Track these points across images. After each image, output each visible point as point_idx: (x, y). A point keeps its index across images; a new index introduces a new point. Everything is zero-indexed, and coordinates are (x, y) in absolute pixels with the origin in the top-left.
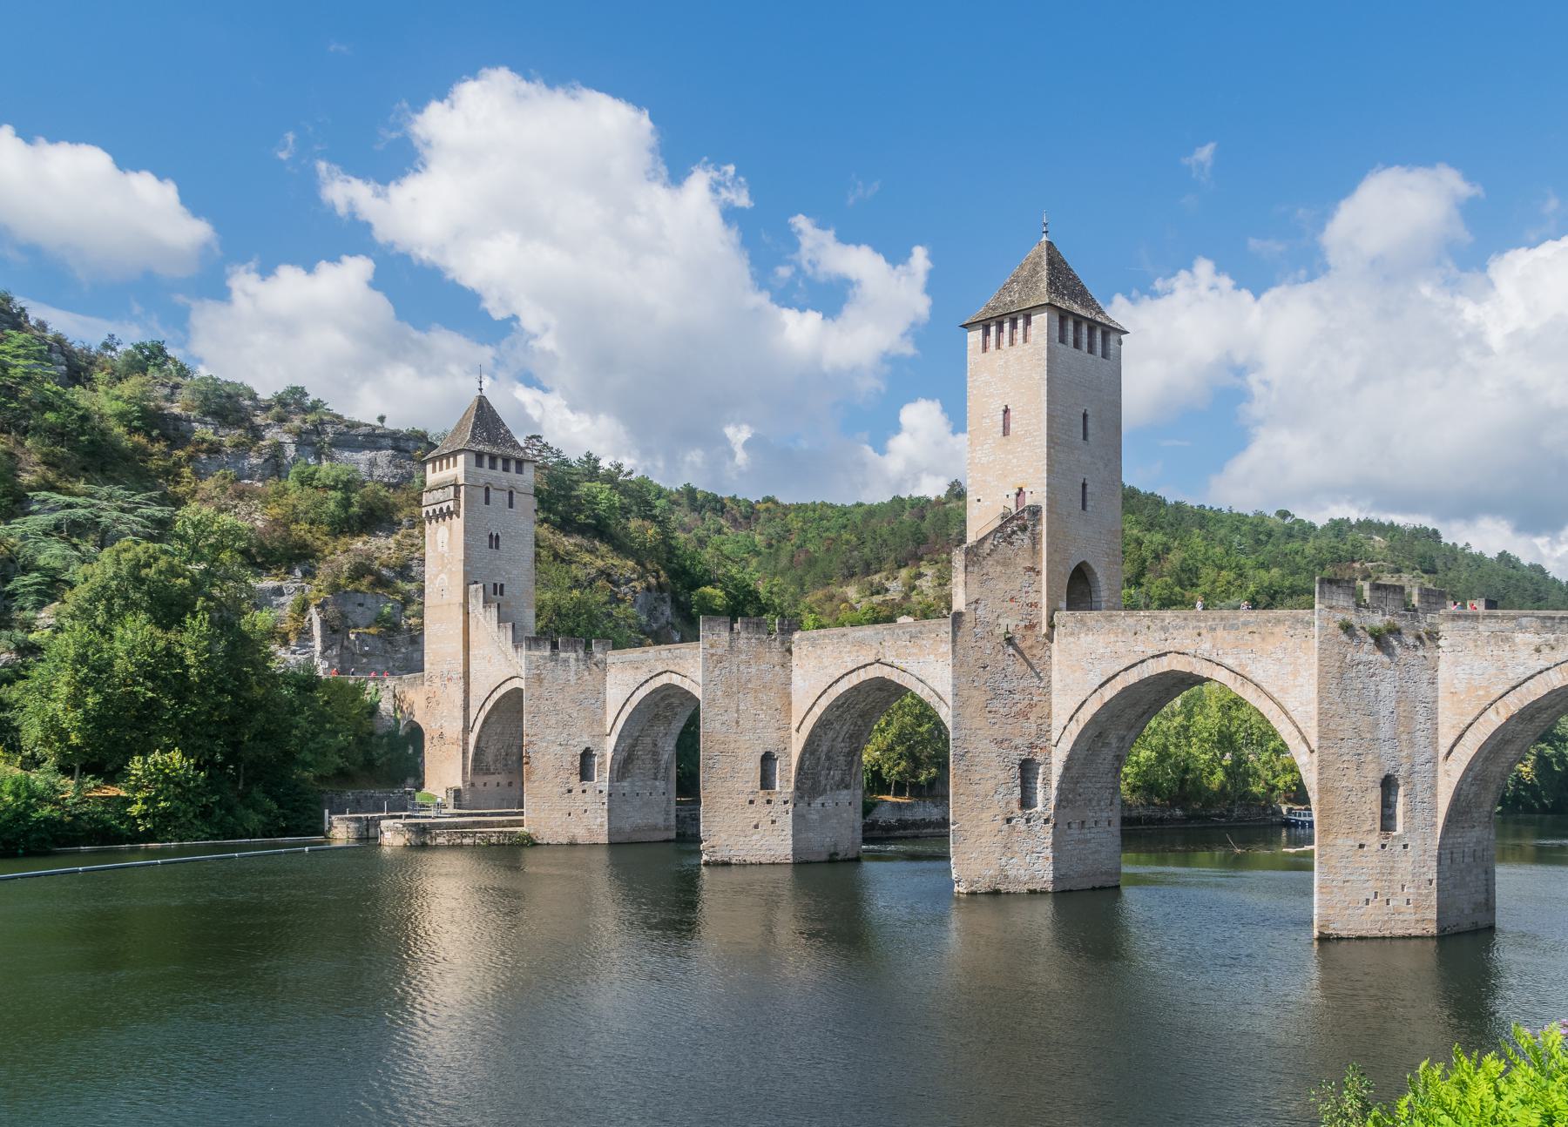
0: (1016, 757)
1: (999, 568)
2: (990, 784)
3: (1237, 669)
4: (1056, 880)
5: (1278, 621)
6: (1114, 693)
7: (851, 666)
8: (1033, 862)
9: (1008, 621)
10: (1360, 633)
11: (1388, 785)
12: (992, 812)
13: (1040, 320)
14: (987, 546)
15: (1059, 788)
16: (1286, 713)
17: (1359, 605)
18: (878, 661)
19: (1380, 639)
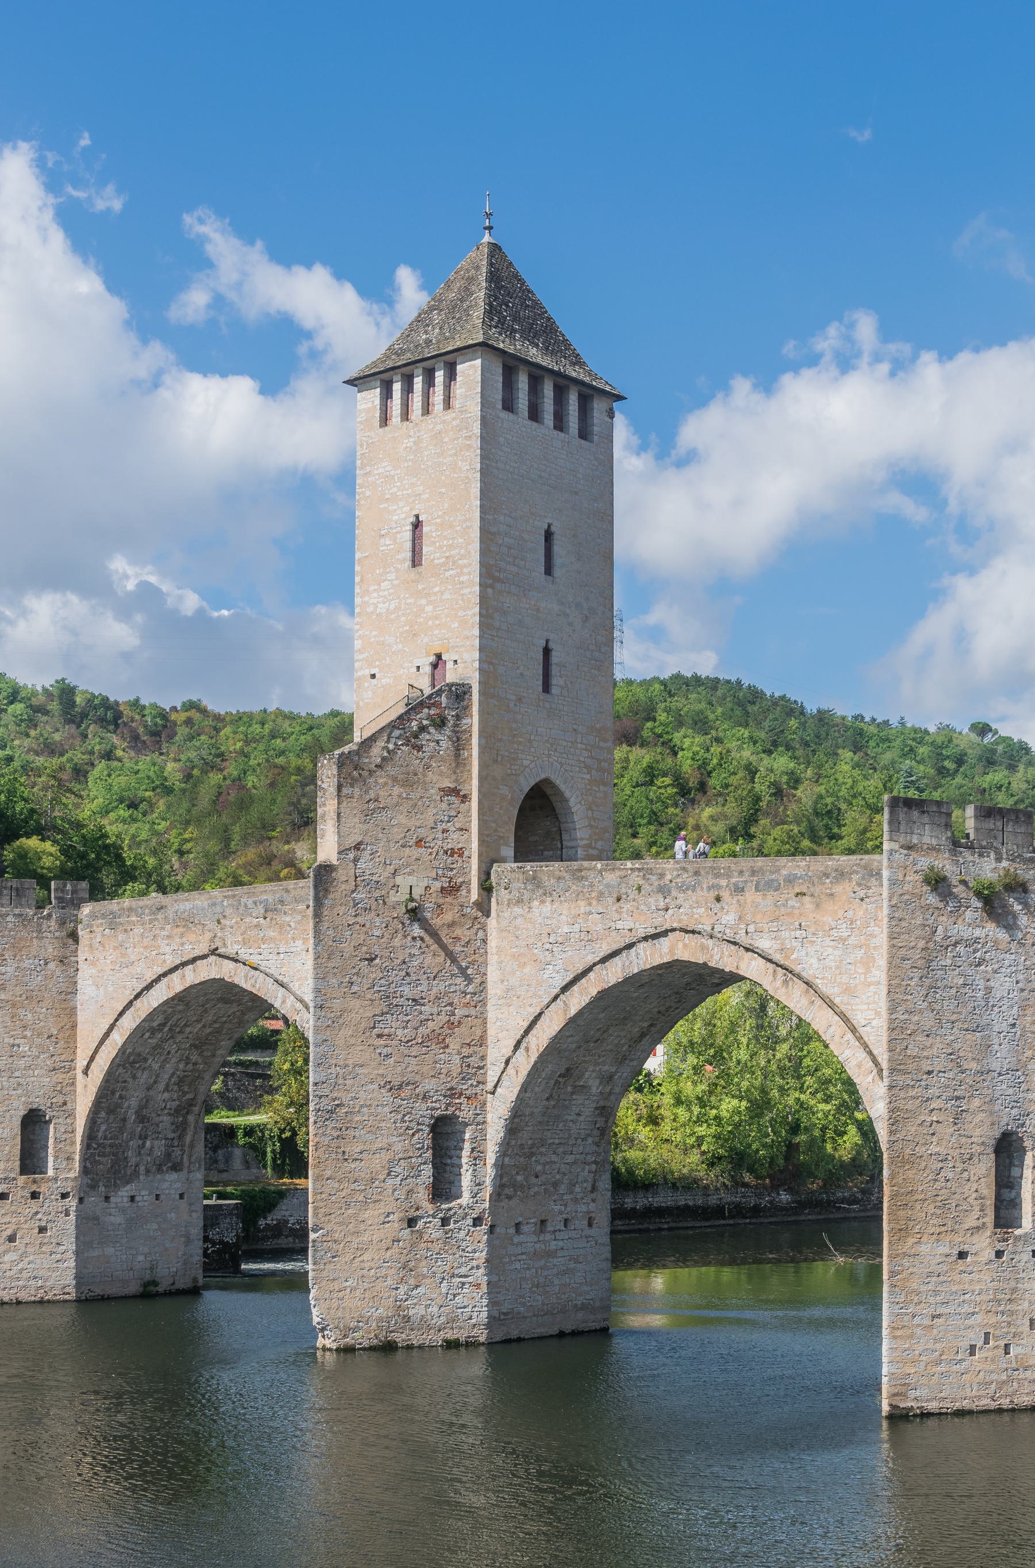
0: (424, 1112)
1: (397, 790)
2: (378, 1162)
3: (777, 957)
4: (493, 1322)
5: (841, 875)
6: (585, 1000)
7: (171, 961)
8: (454, 1294)
9: (412, 880)
10: (959, 890)
11: (1007, 1149)
12: (382, 1208)
13: (470, 371)
14: (377, 752)
15: (499, 1165)
16: (854, 1030)
17: (957, 844)
18: (214, 952)
19: (992, 903)
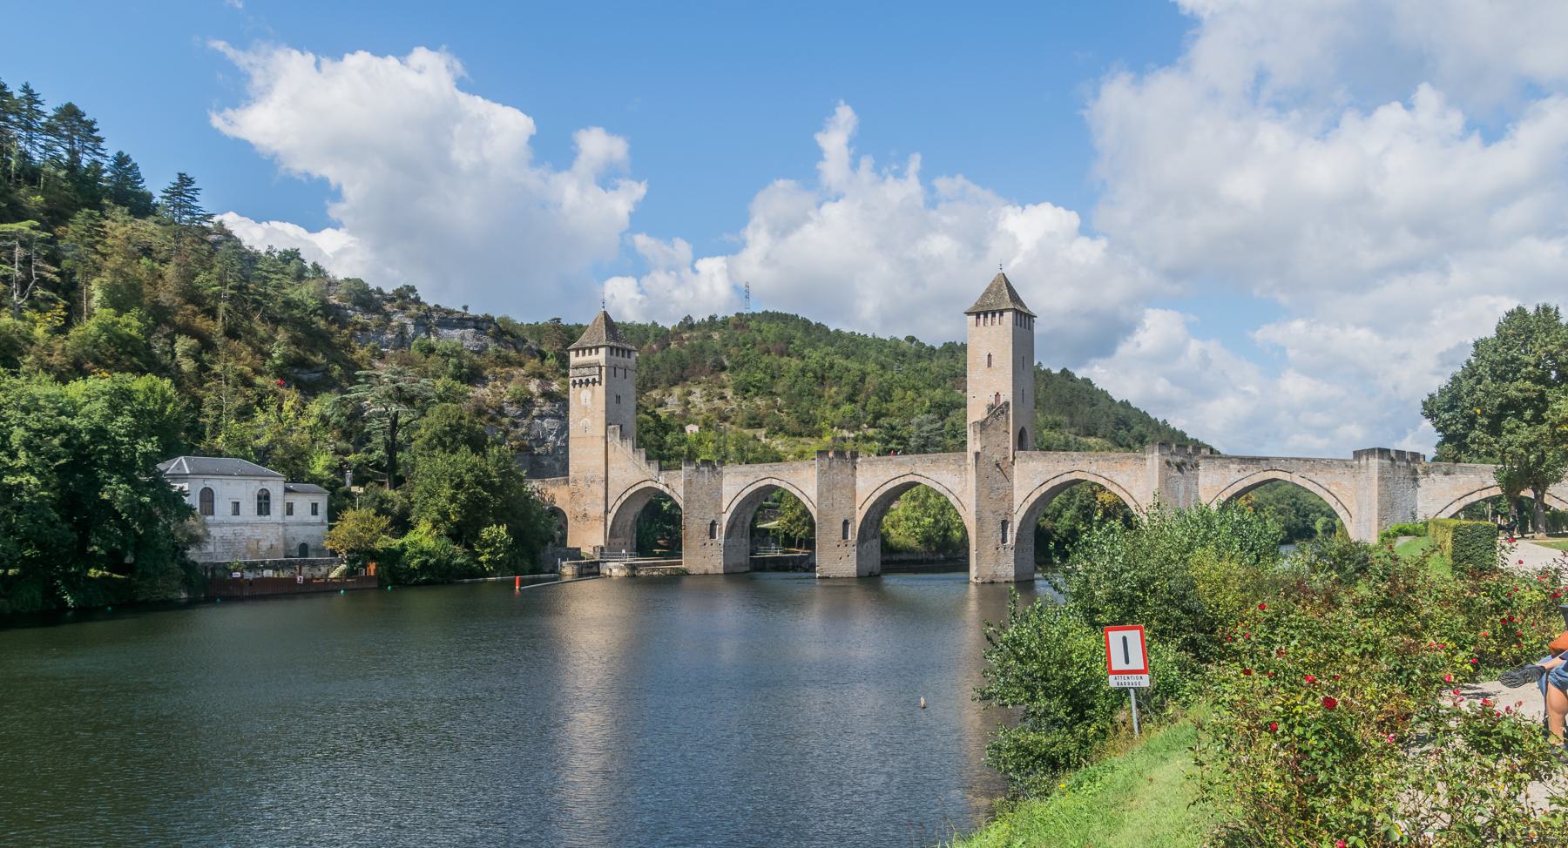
0: (1000, 519)
19: (1180, 467)
